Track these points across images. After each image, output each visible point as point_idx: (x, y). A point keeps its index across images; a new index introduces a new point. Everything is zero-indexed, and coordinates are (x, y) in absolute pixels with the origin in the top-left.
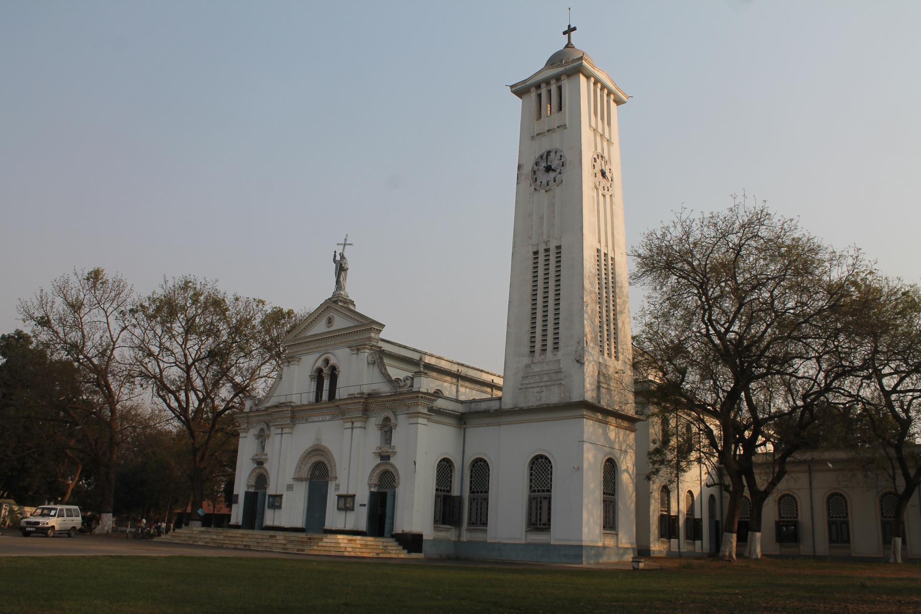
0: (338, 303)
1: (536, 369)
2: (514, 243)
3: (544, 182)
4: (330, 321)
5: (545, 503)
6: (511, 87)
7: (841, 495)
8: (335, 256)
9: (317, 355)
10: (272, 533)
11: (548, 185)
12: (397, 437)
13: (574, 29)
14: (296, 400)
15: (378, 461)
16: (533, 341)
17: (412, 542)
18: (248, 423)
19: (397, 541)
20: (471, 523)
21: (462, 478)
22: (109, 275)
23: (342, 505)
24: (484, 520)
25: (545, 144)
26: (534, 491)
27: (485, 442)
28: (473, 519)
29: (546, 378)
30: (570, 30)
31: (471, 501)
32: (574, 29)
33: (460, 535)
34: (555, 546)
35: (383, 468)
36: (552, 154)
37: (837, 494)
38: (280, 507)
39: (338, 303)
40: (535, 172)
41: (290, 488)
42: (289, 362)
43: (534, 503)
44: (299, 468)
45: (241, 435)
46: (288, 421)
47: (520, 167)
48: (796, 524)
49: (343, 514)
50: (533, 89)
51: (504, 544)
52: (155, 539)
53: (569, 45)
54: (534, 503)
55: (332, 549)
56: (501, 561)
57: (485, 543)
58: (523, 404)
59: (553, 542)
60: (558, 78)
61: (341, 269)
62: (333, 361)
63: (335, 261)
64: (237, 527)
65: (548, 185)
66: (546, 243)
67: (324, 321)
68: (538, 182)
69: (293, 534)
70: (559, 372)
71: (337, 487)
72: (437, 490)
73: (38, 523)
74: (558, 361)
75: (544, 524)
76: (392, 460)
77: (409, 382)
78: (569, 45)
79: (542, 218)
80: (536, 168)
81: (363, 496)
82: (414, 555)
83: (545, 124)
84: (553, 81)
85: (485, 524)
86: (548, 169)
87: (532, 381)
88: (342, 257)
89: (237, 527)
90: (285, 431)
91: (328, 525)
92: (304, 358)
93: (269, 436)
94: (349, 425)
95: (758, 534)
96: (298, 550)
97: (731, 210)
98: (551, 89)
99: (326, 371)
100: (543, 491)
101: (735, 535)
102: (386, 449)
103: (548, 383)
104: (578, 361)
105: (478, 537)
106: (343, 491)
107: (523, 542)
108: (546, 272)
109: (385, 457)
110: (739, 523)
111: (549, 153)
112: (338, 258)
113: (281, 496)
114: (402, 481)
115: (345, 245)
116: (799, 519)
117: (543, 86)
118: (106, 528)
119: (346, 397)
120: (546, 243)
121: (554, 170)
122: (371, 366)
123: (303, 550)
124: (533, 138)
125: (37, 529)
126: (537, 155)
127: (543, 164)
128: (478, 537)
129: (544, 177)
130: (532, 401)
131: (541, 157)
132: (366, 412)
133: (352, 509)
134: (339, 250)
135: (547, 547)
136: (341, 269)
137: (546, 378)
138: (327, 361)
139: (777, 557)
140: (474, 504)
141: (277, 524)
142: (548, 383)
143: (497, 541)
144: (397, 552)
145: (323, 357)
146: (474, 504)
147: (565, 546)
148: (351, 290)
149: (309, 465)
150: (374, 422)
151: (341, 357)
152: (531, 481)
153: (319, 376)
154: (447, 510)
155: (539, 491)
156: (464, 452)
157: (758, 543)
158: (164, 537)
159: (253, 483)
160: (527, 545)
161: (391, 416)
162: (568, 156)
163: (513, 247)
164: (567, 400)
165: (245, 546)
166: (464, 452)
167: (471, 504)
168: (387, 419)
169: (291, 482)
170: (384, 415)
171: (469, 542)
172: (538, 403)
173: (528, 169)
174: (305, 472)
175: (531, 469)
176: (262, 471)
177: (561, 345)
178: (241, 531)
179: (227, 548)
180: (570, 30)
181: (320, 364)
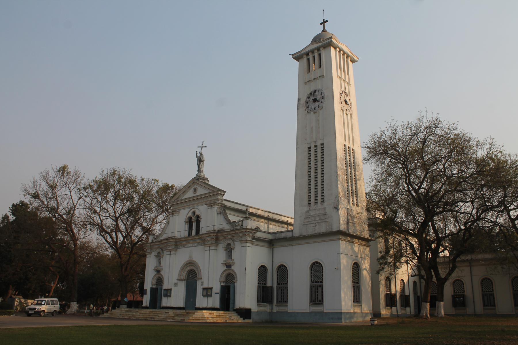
0: (199, 180)
1: (312, 213)
3: (313, 108)
4: (195, 190)
5: (320, 289)
6: (292, 55)
7: (489, 279)
8: (197, 154)
9: (189, 209)
10: (166, 310)
11: (315, 109)
12: (235, 255)
13: (327, 21)
14: (177, 235)
15: (225, 268)
16: (309, 197)
17: (245, 313)
18: (151, 249)
19: (237, 313)
20: (278, 302)
21: (272, 277)
22: (71, 168)
23: (205, 293)
24: (285, 300)
25: (313, 87)
26: (313, 282)
27: (285, 255)
28: (280, 299)
29: (318, 218)
30: (324, 22)
31: (278, 289)
32: (327, 21)
33: (272, 309)
34: (326, 313)
35: (228, 272)
36: (317, 92)
37: (487, 278)
38: (170, 296)
39: (199, 180)
40: (307, 103)
41: (176, 285)
42: (173, 214)
43: (313, 289)
44: (180, 274)
45: (147, 256)
46: (174, 247)
47: (299, 100)
48: (464, 296)
49: (206, 298)
50: (305, 56)
51: (298, 313)
52: (101, 316)
53: (324, 31)
54: (313, 289)
55: (200, 318)
56: (296, 322)
57: (287, 312)
58: (305, 234)
59: (325, 311)
60: (318, 49)
61: (200, 161)
62: (197, 213)
63: (197, 156)
64: (146, 308)
65: (315, 109)
66: (315, 142)
67: (192, 190)
68: (309, 108)
69: (178, 311)
70: (325, 214)
71: (202, 283)
72: (258, 283)
73: (35, 309)
74: (325, 208)
75: (320, 301)
76: (232, 268)
77: (240, 223)
78: (324, 31)
79: (312, 128)
80: (308, 100)
81: (217, 288)
82: (247, 321)
83: (312, 76)
84: (316, 51)
85: (286, 302)
86: (315, 100)
87: (310, 220)
88: (201, 154)
89: (146, 308)
90: (172, 253)
91: (198, 305)
92: (181, 212)
93: (163, 256)
94: (208, 248)
95: (442, 303)
96: (181, 320)
97: (419, 119)
98: (315, 55)
100: (318, 282)
101: (428, 304)
102: (229, 261)
103: (319, 221)
104: (336, 208)
105: (282, 309)
106: (205, 286)
107: (308, 311)
108: (315, 158)
109: (228, 266)
110: (431, 297)
111: (315, 91)
112: (199, 155)
113: (171, 290)
114: (238, 279)
115: (202, 147)
116: (466, 293)
117: (310, 54)
118: (73, 311)
119: (205, 232)
120: (315, 142)
121: (318, 101)
122: (219, 215)
123: (184, 320)
124: (305, 83)
125: (35, 312)
127: (312, 98)
128: (282, 309)
129: (312, 105)
130: (310, 231)
131: (311, 94)
132: (217, 240)
133: (211, 296)
134: (199, 150)
135: (322, 314)
136: (200, 161)
137: (318, 218)
138: (194, 213)
139: (453, 315)
140: (280, 291)
141: (169, 305)
142: (319, 221)
143: (293, 311)
144: (237, 319)
145: (192, 211)
146: (280, 291)
147: (332, 313)
148: (206, 172)
149: (186, 272)
150: (222, 246)
151: (202, 210)
152: (311, 276)
153: (190, 221)
154: (264, 294)
155: (316, 282)
156: (273, 261)
157: (442, 308)
158: (106, 315)
159: (155, 283)
160: (311, 313)
161: (230, 242)
162: (326, 93)
163: (297, 145)
164: (330, 230)
165: (151, 318)
166: (273, 261)
167: (278, 290)
168: (229, 245)
169: (176, 281)
170: (227, 242)
171: (277, 312)
172: (314, 233)
173: (303, 101)
174: (184, 276)
175: (311, 270)
176: (160, 276)
177: (325, 199)
178: (149, 310)
179: (141, 320)
180: (324, 22)
181: (190, 214)
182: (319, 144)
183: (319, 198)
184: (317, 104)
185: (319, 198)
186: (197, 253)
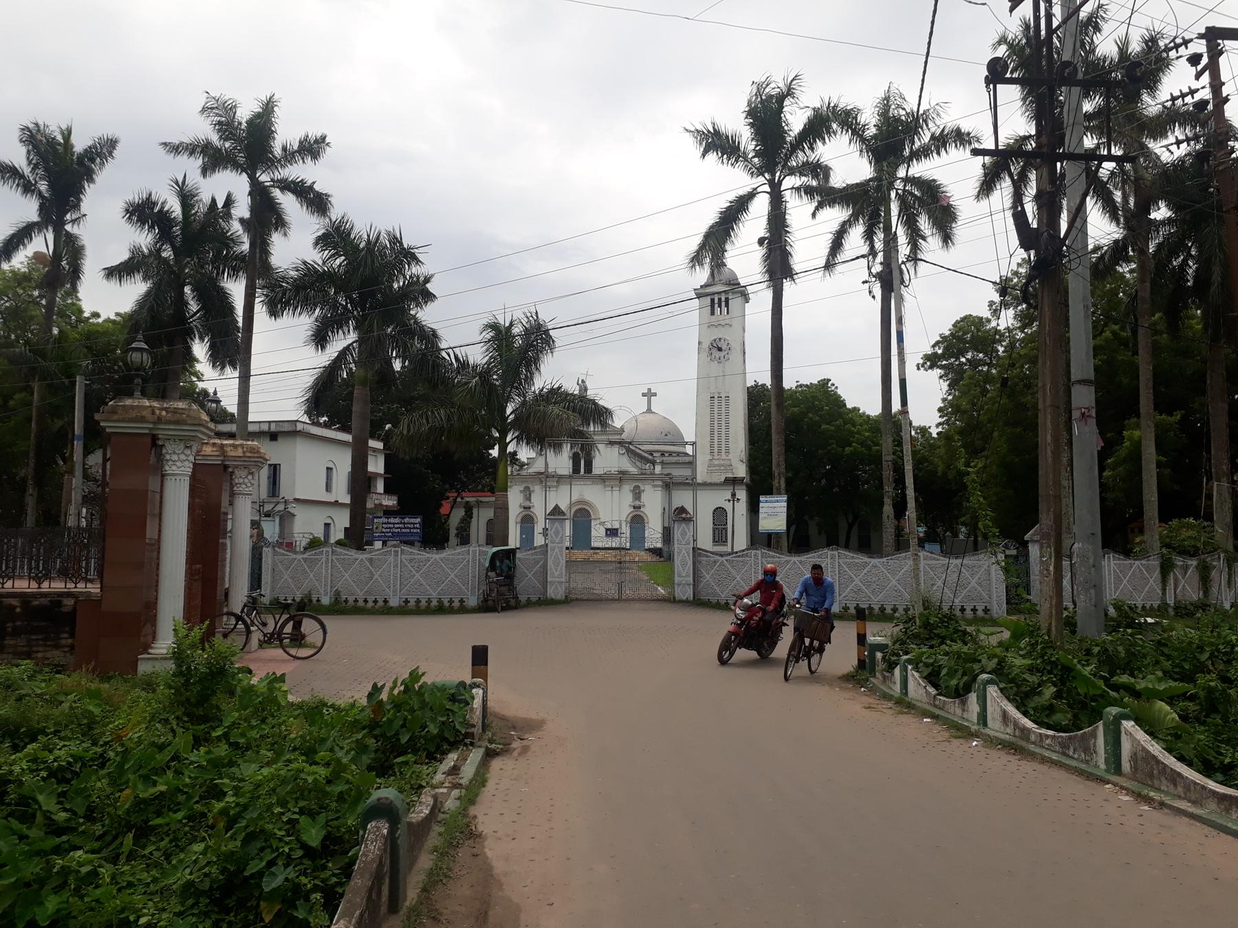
1: (716, 462)
12: (644, 497)
16: (712, 446)
27: (683, 498)
81: (626, 530)
86: (720, 349)
91: (594, 544)
102: (637, 503)
129: (716, 354)
144: (648, 557)
150: (627, 488)
153: (575, 459)
162: (733, 344)
173: (706, 345)
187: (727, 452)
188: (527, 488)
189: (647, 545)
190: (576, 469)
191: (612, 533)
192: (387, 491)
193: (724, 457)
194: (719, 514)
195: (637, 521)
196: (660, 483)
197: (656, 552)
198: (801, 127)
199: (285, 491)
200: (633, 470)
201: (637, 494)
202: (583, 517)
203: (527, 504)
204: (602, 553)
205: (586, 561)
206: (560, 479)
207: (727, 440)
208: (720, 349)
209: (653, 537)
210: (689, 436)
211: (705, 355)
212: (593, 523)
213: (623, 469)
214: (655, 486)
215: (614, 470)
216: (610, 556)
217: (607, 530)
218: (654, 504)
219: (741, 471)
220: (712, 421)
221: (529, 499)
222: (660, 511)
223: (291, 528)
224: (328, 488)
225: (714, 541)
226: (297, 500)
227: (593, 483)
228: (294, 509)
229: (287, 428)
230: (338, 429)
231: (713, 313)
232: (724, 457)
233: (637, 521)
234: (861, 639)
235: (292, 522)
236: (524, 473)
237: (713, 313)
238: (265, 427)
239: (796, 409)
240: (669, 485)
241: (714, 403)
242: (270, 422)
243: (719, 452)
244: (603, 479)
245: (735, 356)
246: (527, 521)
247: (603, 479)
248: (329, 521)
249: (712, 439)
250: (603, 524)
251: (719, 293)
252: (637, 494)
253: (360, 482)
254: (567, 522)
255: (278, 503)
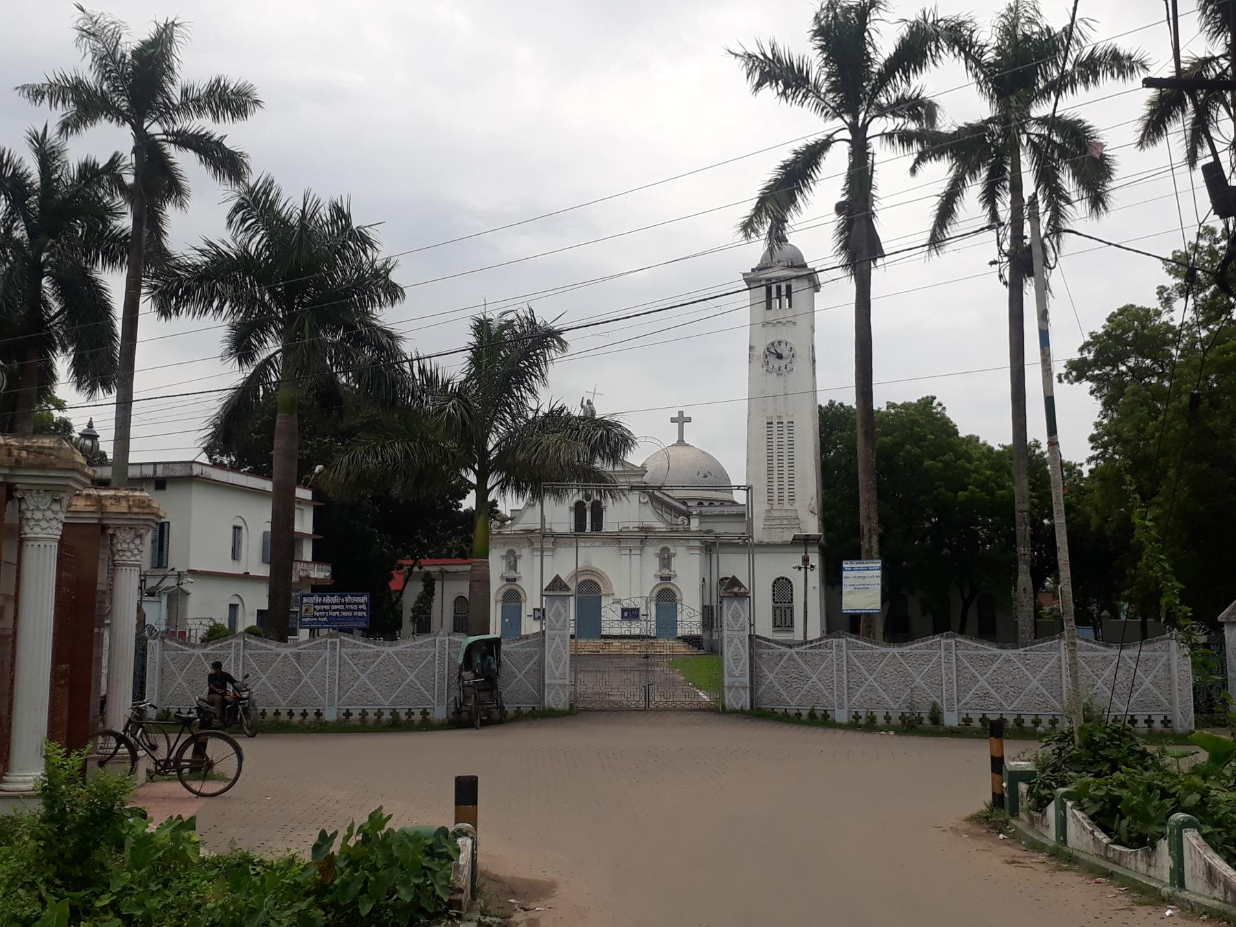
1: (776, 514)
2: (749, 412)
5: (788, 611)
12: (675, 563)
15: (659, 581)
25: (774, 335)
36: (783, 345)
43: (778, 612)
47: (751, 348)
54: (778, 612)
58: (766, 540)
83: (770, 316)
86: (780, 356)
88: (589, 403)
91: (604, 633)
99: (588, 504)
102: (666, 572)
111: (780, 342)
126: (769, 341)
129: (775, 363)
150: (652, 551)
153: (579, 509)
162: (797, 350)
168: (665, 550)
172: (780, 541)
173: (760, 350)
182: (785, 421)
183: (786, 495)
184: (782, 363)
185: (786, 495)
186: (599, 558)
187: (792, 499)
188: (511, 552)
189: (680, 632)
190: (580, 525)
191: (631, 614)
192: (317, 558)
193: (787, 506)
194: (782, 586)
195: (666, 598)
196: (697, 544)
197: (691, 640)
198: (892, 51)
199: (176, 560)
200: (660, 525)
201: (666, 559)
202: (589, 592)
203: (512, 574)
204: (616, 643)
205: (595, 655)
206: (557, 539)
207: (791, 482)
208: (780, 356)
209: (689, 620)
210: (737, 475)
211: (758, 364)
212: (603, 599)
213: (645, 524)
214: (690, 548)
215: (632, 526)
216: (627, 647)
217: (623, 610)
218: (689, 572)
219: (812, 527)
220: (770, 456)
221: (514, 567)
222: (697, 583)
223: (185, 612)
224: (235, 555)
225: (775, 625)
226: (193, 573)
227: (604, 545)
228: (189, 585)
229: (179, 471)
230: (250, 473)
231: (769, 307)
232: (787, 506)
233: (666, 598)
234: (997, 764)
235: (185, 603)
236: (506, 531)
237: (769, 307)
238: (149, 471)
239: (888, 439)
240: (710, 547)
241: (771, 432)
242: (155, 464)
243: (781, 500)
244: (618, 539)
245: (801, 365)
246: (513, 597)
247: (618, 539)
248: (236, 601)
249: (770, 481)
250: (618, 602)
251: (779, 280)
252: (666, 559)
253: (281, 545)
254: (572, 599)
255: (165, 577)
